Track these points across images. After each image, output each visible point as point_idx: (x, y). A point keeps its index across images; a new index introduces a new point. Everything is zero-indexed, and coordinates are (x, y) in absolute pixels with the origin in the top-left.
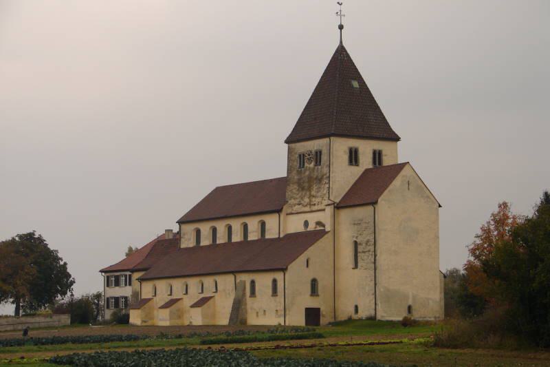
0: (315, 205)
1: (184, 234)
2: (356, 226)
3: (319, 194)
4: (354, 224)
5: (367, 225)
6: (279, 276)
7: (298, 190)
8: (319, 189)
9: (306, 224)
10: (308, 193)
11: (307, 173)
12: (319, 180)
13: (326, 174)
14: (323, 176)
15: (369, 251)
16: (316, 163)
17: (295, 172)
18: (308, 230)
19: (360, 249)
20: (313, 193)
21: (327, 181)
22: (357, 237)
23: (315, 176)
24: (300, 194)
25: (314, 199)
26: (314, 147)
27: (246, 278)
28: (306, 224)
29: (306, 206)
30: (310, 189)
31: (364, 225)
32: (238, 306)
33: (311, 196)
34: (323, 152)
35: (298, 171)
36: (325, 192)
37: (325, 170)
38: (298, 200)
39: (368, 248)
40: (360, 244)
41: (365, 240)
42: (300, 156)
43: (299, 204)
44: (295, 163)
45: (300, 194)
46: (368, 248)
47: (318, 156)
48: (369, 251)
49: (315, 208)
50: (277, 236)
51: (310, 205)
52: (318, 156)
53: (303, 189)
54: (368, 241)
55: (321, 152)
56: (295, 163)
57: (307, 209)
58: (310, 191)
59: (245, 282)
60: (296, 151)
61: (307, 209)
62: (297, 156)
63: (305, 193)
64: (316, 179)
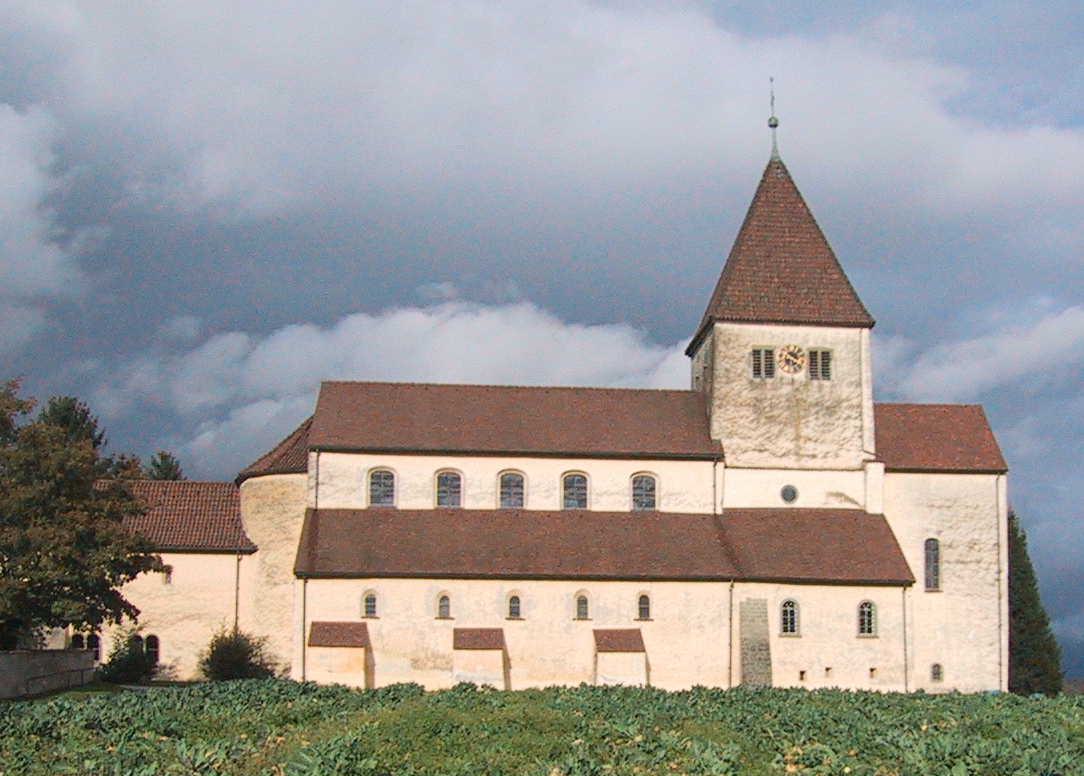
0: (814, 456)
1: (331, 477)
2: (936, 512)
3: (829, 437)
4: (932, 506)
5: (970, 511)
6: (884, 598)
7: (757, 420)
8: (827, 427)
9: (789, 494)
10: (790, 432)
11: (786, 390)
12: (831, 410)
13: (848, 400)
14: (839, 402)
15: (979, 562)
16: (813, 374)
17: (745, 382)
18: (799, 503)
19: (945, 554)
20: (805, 432)
21: (854, 415)
22: (939, 533)
23: (811, 400)
24: (763, 430)
25: (810, 445)
26: (807, 341)
27: (773, 595)
28: (789, 494)
29: (784, 455)
30: (795, 422)
31: (963, 512)
32: (756, 653)
33: (798, 438)
34: (836, 355)
35: (751, 382)
36: (848, 434)
37: (845, 391)
38: (757, 442)
39: (974, 555)
40: (950, 546)
41: (968, 539)
42: (756, 353)
43: (761, 451)
44: (742, 365)
45: (763, 430)
46: (974, 555)
47: (820, 363)
48: (979, 562)
49: (811, 463)
50: (709, 510)
51: (797, 454)
52: (820, 363)
53: (771, 419)
54: (972, 545)
55: (826, 356)
56: (742, 365)
57: (790, 462)
58: (797, 427)
59: (764, 604)
60: (743, 341)
61: (790, 462)
62: (749, 350)
63: (781, 432)
64: (817, 404)
